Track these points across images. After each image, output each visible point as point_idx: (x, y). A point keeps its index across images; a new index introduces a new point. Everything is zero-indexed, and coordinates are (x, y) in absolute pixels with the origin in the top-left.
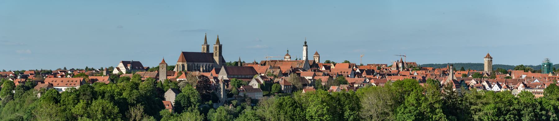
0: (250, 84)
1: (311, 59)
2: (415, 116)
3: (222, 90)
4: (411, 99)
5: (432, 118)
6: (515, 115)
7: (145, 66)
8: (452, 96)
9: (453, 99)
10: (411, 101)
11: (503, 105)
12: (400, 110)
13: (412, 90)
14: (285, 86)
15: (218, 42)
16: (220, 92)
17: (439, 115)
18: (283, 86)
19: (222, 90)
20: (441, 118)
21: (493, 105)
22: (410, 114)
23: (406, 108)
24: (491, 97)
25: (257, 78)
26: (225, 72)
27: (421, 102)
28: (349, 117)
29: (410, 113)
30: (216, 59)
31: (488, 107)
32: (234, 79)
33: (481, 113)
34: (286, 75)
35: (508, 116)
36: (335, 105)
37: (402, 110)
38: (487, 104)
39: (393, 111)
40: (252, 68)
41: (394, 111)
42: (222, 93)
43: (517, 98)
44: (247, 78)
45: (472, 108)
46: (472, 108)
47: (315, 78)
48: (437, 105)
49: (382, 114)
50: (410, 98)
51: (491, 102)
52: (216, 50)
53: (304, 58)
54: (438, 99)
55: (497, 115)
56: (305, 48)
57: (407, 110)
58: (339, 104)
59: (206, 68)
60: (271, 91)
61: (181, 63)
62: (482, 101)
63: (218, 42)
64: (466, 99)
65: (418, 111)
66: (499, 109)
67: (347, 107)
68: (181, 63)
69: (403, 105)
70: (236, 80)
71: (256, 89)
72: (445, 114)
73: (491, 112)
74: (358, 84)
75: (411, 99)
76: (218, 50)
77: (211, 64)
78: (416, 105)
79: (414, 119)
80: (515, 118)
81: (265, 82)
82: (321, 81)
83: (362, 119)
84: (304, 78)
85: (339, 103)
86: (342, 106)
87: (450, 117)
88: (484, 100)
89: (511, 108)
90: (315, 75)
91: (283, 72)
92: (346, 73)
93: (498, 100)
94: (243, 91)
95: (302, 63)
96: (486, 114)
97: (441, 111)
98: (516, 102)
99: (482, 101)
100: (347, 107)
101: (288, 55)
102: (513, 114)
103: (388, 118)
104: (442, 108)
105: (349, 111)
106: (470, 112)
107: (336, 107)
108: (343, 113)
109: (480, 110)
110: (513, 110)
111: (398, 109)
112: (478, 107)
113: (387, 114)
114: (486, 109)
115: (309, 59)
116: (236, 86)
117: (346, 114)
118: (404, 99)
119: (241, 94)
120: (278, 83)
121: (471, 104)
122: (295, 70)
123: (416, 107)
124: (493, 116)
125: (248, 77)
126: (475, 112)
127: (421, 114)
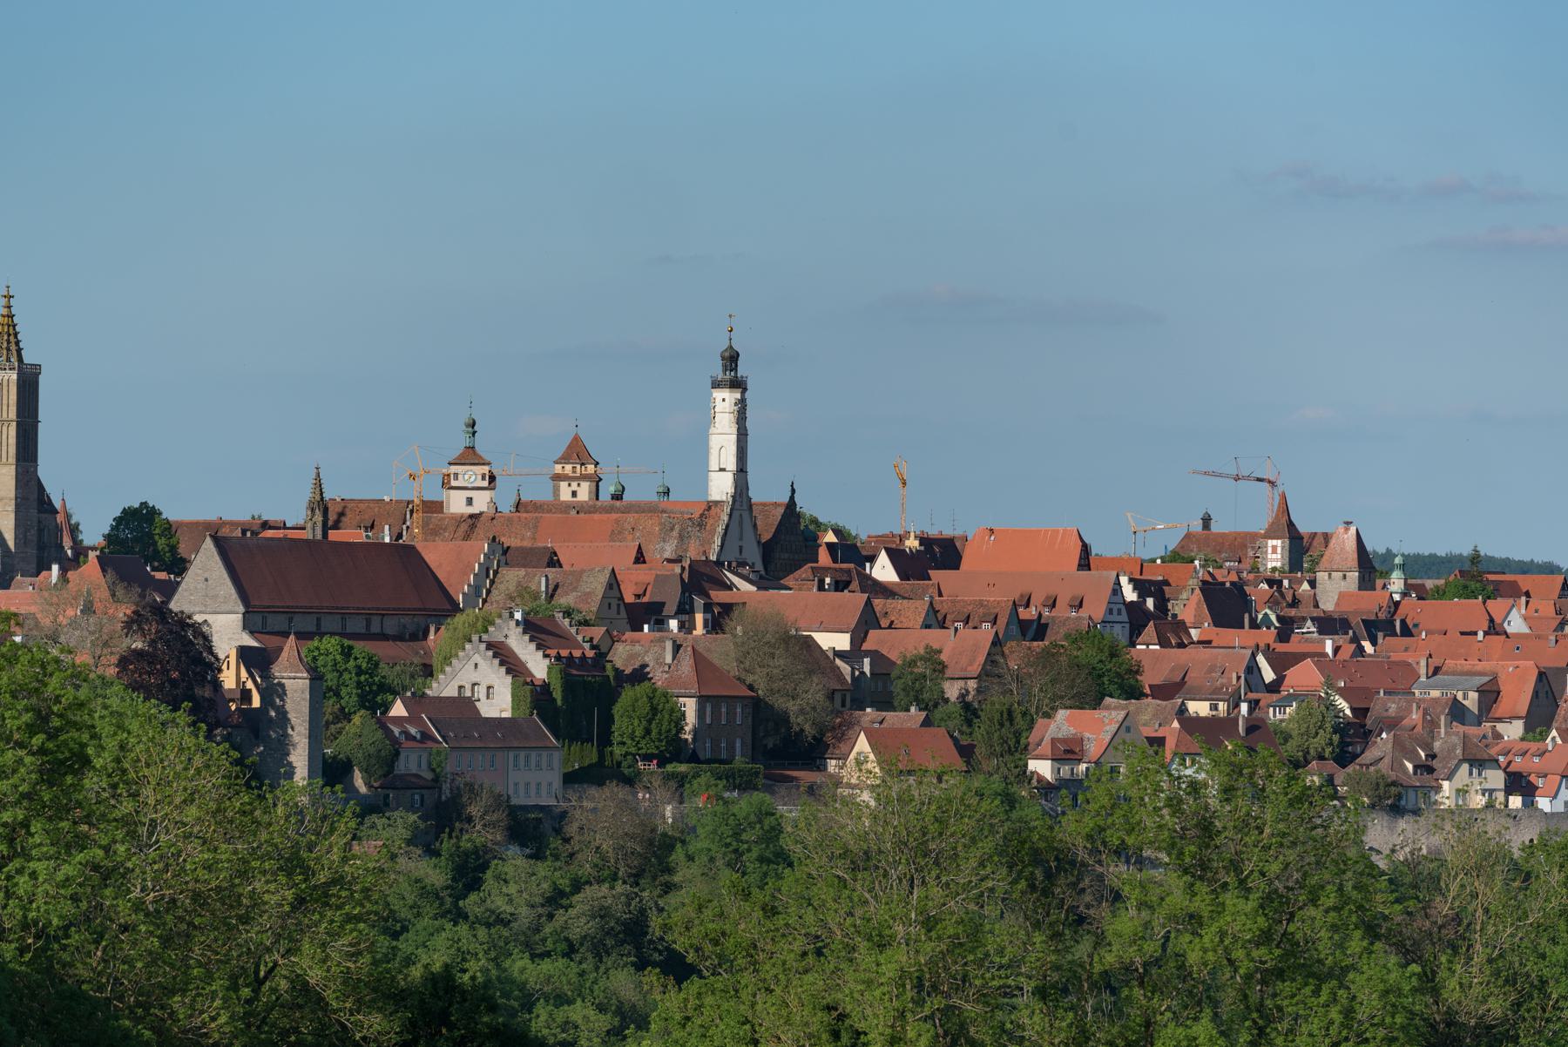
0: (445, 687)
1: (767, 491)
14: (703, 700)
16: (282, 747)
18: (690, 707)
25: (494, 634)
26: (227, 588)
32: (331, 644)
34: (646, 613)
40: (406, 555)
42: (299, 759)
44: (383, 637)
47: (874, 640)
53: (721, 487)
56: (725, 400)
60: (605, 740)
70: (347, 653)
71: (499, 722)
74: (1212, 696)
81: (565, 665)
82: (940, 668)
84: (810, 644)
90: (868, 622)
91: (629, 598)
92: (1063, 611)
94: (426, 736)
95: (701, 525)
101: (470, 456)
115: (757, 495)
116: (350, 697)
119: (411, 763)
120: (640, 675)
122: (700, 581)
125: (391, 626)
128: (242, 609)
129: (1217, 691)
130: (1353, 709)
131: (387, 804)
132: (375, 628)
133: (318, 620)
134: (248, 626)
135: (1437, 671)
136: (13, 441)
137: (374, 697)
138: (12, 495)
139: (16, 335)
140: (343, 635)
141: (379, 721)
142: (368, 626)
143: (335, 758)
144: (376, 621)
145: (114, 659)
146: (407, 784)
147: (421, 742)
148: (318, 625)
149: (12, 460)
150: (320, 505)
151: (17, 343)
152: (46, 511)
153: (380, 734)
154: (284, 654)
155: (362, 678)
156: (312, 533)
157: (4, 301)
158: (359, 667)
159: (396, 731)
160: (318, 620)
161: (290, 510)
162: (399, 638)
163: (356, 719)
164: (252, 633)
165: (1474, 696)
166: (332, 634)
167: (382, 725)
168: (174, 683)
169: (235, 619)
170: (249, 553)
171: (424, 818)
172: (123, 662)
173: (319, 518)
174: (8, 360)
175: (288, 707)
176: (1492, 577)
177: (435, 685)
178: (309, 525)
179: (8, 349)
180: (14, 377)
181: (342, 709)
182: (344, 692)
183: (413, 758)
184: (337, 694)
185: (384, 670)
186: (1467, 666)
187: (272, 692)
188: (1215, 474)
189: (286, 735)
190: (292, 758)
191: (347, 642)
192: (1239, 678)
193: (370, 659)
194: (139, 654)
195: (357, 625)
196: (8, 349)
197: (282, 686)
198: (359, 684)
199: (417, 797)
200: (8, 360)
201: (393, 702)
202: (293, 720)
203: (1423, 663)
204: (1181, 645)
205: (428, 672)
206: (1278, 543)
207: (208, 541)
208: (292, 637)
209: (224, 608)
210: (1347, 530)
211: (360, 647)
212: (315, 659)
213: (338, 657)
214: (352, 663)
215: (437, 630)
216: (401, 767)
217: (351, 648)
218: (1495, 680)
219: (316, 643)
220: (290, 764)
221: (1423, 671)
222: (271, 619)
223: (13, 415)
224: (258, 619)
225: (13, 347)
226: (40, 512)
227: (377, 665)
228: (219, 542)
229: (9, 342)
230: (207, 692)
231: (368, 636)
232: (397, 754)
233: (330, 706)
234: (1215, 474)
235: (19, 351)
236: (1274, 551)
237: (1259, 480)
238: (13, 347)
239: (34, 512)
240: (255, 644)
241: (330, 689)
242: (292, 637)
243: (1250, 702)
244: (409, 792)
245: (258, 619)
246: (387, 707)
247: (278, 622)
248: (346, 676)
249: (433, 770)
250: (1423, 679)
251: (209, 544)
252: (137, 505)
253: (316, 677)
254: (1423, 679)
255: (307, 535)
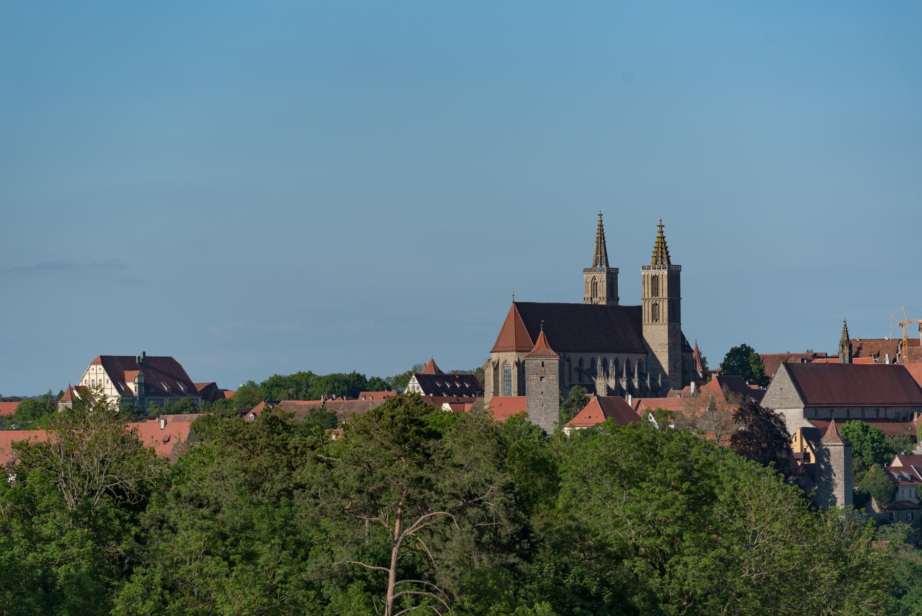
3: (839, 478)
7: (198, 376)
15: (662, 251)
16: (829, 486)
19: (839, 478)
26: (794, 394)
30: (656, 335)
32: (856, 425)
40: (899, 372)
42: (839, 493)
44: (886, 420)
52: (655, 292)
59: (618, 375)
61: (511, 358)
63: (662, 251)
68: (511, 358)
70: (866, 430)
76: (664, 292)
77: (635, 358)
94: (914, 478)
116: (868, 456)
119: (905, 494)
125: (891, 414)
128: (803, 405)
131: (892, 519)
132: (882, 415)
133: (848, 411)
134: (806, 416)
136: (666, 310)
137: (882, 456)
138: (667, 342)
139: (666, 248)
140: (862, 419)
141: (885, 470)
142: (878, 411)
143: (860, 492)
144: (882, 411)
145: (729, 437)
146: (903, 507)
147: (911, 481)
148: (848, 414)
149: (666, 321)
150: (847, 343)
151: (667, 253)
152: (686, 351)
153: (886, 477)
154: (829, 432)
155: (875, 445)
156: (843, 360)
157: (659, 229)
158: (873, 438)
159: (896, 475)
160: (848, 411)
161: (829, 346)
162: (896, 420)
163: (872, 469)
164: (809, 419)
166: (856, 419)
167: (888, 472)
168: (764, 450)
169: (799, 412)
170: (806, 373)
171: (913, 527)
172: (734, 439)
173: (846, 351)
174: (662, 263)
175: (831, 463)
177: (918, 448)
178: (841, 355)
179: (662, 257)
180: (666, 273)
181: (864, 463)
182: (864, 453)
183: (907, 491)
184: (860, 454)
185: (888, 439)
187: (822, 454)
189: (831, 479)
190: (835, 493)
191: (865, 424)
193: (879, 434)
194: (743, 433)
195: (870, 413)
196: (662, 257)
197: (828, 450)
198: (873, 449)
199: (909, 514)
200: (662, 263)
201: (894, 458)
202: (835, 470)
205: (914, 440)
207: (782, 365)
208: (833, 421)
209: (793, 405)
211: (872, 426)
212: (846, 434)
213: (861, 433)
214: (868, 436)
215: (919, 415)
216: (900, 497)
217: (867, 427)
219: (847, 425)
220: (834, 496)
222: (820, 411)
223: (665, 295)
224: (813, 411)
225: (665, 256)
226: (683, 351)
227: (883, 437)
228: (788, 367)
229: (662, 252)
230: (784, 455)
231: (878, 420)
232: (897, 489)
233: (856, 461)
235: (668, 257)
238: (665, 256)
239: (679, 351)
240: (811, 426)
241: (856, 452)
242: (833, 421)
244: (905, 512)
245: (813, 411)
246: (890, 461)
247: (824, 413)
248: (865, 444)
249: (918, 498)
251: (782, 368)
252: (739, 346)
253: (848, 445)
255: (840, 361)
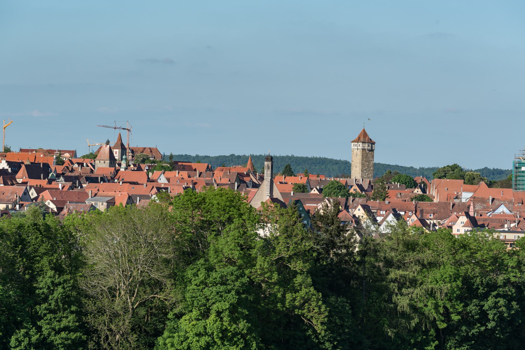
2: (238, 293)
4: (225, 244)
5: (283, 300)
6: (509, 299)
8: (337, 241)
9: (340, 248)
10: (227, 252)
11: (477, 270)
12: (196, 275)
13: (230, 220)
17: (302, 293)
20: (306, 301)
21: (450, 270)
22: (222, 288)
23: (210, 269)
24: (444, 246)
27: (253, 252)
28: (52, 292)
29: (223, 283)
31: (436, 273)
33: (418, 291)
35: (491, 301)
36: (11, 255)
37: (202, 275)
38: (432, 265)
39: (173, 276)
41: (178, 278)
43: (515, 253)
45: (392, 276)
46: (392, 276)
48: (297, 265)
49: (142, 283)
50: (222, 240)
51: (445, 259)
54: (301, 248)
55: (460, 298)
57: (214, 275)
58: (22, 254)
62: (421, 256)
64: (376, 251)
65: (245, 280)
66: (467, 281)
67: (45, 261)
69: (202, 261)
72: (317, 290)
73: (446, 287)
75: (225, 244)
78: (240, 262)
79: (234, 300)
80: (509, 307)
83: (87, 296)
85: (22, 249)
86: (31, 259)
87: (333, 299)
88: (427, 256)
89: (500, 279)
93: (463, 255)
96: (431, 294)
97: (309, 280)
98: (512, 263)
99: (421, 256)
100: (45, 261)
102: (504, 296)
103: (161, 296)
104: (310, 272)
105: (51, 273)
106: (387, 288)
107: (13, 263)
108: (33, 278)
109: (413, 283)
110: (505, 285)
111: (189, 273)
112: (409, 274)
113: (158, 285)
114: (432, 279)
117: (43, 283)
118: (207, 246)
121: (389, 263)
123: (240, 267)
124: (450, 300)
126: (400, 289)
127: (252, 287)
129: (9, 201)
130: (57, 208)
135: (96, 195)
165: (105, 204)
176: (180, 164)
186: (105, 193)
188: (106, 127)
192: (17, 196)
203: (90, 192)
204: (13, 184)
206: (117, 150)
210: (106, 146)
218: (114, 199)
221: (90, 195)
234: (106, 127)
236: (116, 152)
237: (123, 129)
243: (20, 205)
250: (90, 198)
254: (90, 198)
